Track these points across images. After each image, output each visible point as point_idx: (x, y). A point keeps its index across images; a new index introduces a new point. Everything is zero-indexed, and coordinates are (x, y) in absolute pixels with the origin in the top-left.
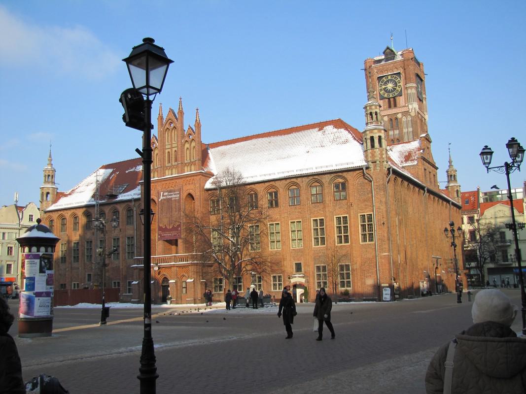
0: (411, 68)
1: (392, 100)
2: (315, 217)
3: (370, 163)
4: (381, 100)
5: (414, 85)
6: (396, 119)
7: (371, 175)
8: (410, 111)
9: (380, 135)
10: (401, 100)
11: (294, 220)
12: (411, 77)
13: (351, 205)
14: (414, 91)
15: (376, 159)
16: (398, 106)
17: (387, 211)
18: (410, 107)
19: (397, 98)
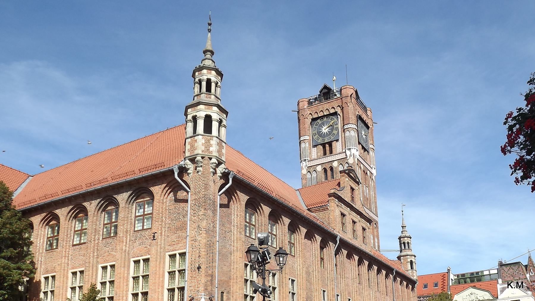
0: (350, 106)
1: (327, 146)
2: (105, 262)
3: (188, 161)
4: (315, 146)
5: (355, 127)
6: (332, 169)
7: (188, 182)
8: (348, 158)
9: (209, 113)
10: (338, 147)
11: (76, 268)
12: (350, 117)
13: (154, 237)
14: (353, 134)
15: (196, 152)
16: (334, 152)
17: (210, 246)
18: (348, 153)
19: (334, 144)
